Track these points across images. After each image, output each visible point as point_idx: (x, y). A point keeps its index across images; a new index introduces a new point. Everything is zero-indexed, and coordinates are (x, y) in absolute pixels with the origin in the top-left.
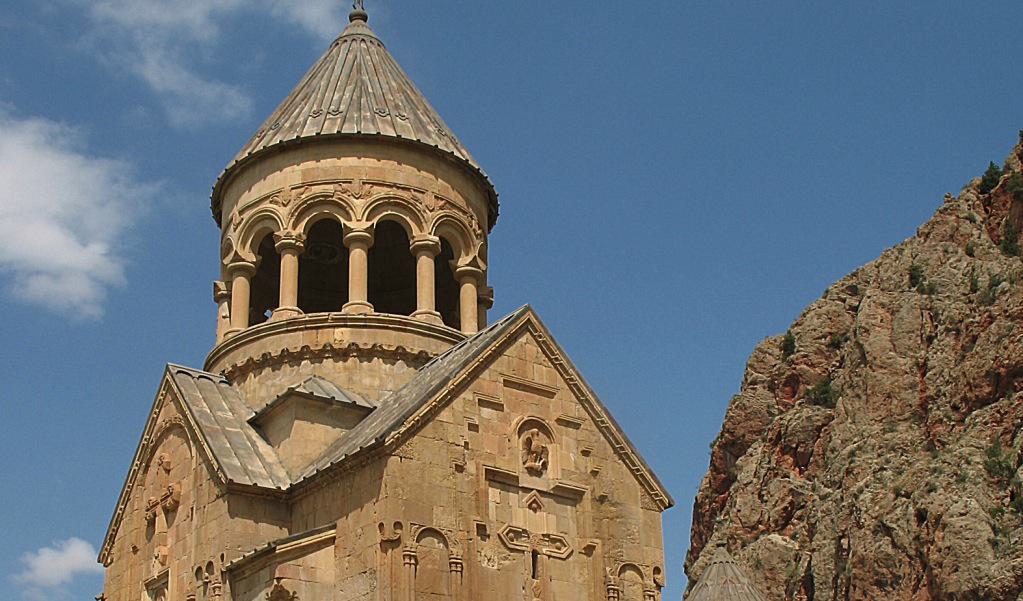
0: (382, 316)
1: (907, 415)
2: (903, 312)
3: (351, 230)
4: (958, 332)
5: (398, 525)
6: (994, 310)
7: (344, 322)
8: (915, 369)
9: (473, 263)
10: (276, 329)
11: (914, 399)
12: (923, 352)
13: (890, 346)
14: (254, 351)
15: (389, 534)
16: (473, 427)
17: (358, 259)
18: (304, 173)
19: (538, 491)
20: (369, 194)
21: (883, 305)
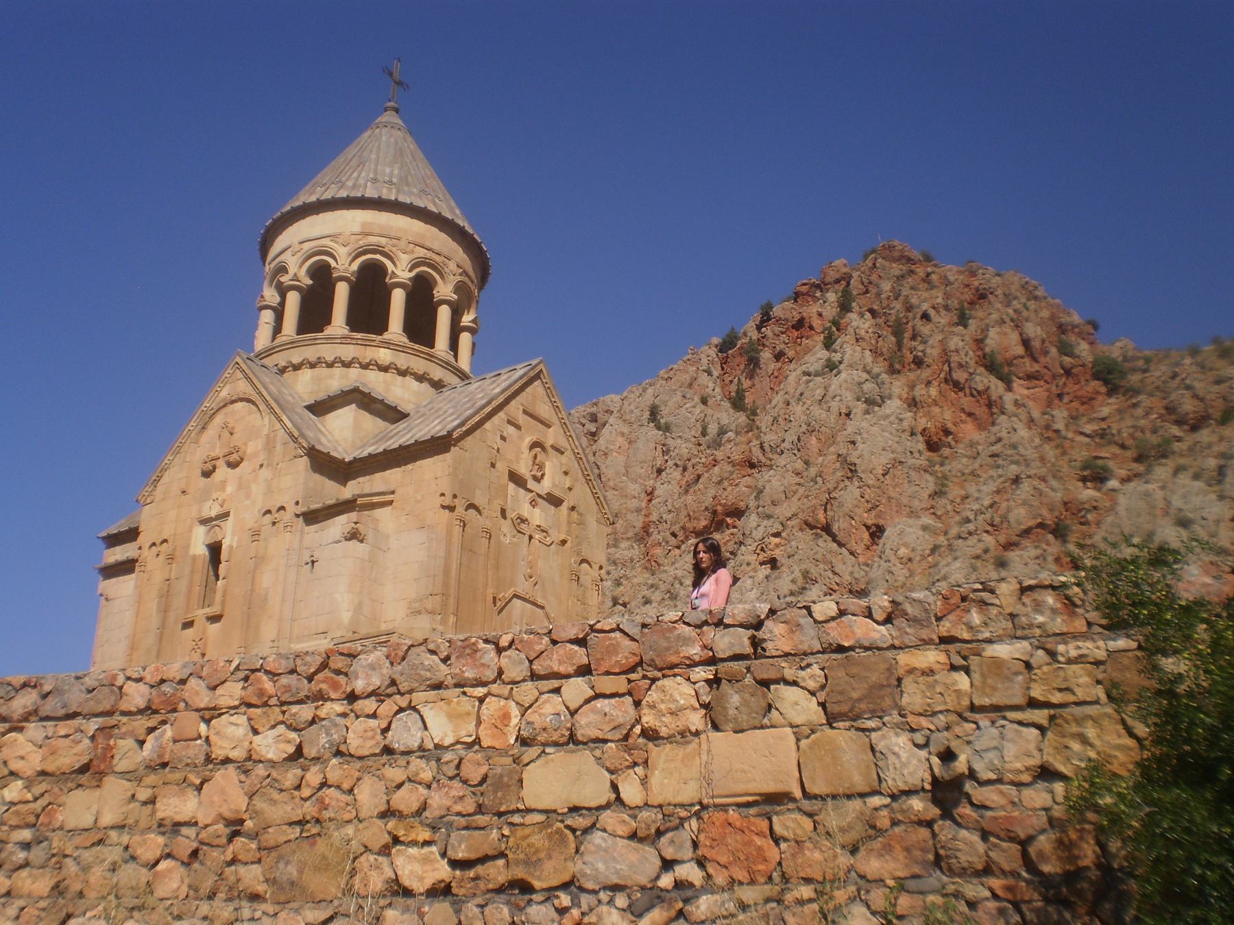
0: (417, 346)
1: (630, 534)
2: (640, 444)
3: (397, 276)
4: (685, 469)
5: (455, 496)
6: (719, 454)
7: (387, 345)
8: (643, 495)
9: (474, 321)
10: (331, 340)
11: (639, 524)
12: (652, 482)
13: (624, 471)
14: (310, 353)
15: (447, 501)
16: (503, 438)
17: (398, 299)
18: (364, 224)
19: (539, 496)
20: (412, 252)
21: (623, 434)
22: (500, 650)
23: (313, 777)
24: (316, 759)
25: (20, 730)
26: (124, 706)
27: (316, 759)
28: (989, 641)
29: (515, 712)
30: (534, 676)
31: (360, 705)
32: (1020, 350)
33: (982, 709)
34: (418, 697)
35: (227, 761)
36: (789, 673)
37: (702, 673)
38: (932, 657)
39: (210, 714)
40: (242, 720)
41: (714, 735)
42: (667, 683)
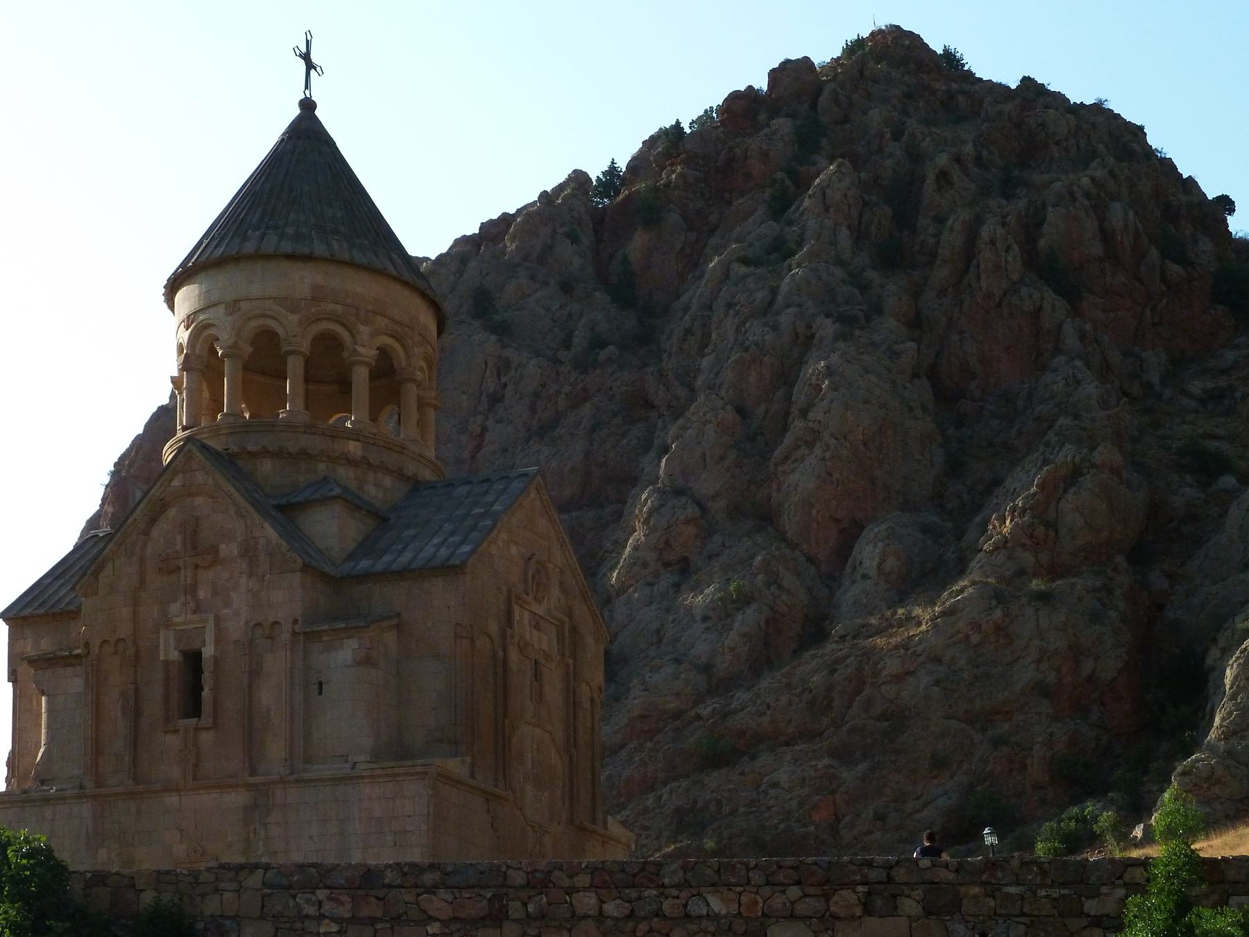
22: (748, 870)
23: (643, 927)
24: (645, 918)
25: (434, 894)
26: (509, 883)
27: (645, 918)
28: (1006, 885)
29: (760, 900)
30: (768, 883)
31: (667, 892)
32: (1097, 249)
33: (1000, 915)
34: (702, 889)
35: (586, 917)
36: (907, 892)
37: (860, 889)
38: (976, 890)
39: (570, 891)
40: (593, 895)
41: (868, 919)
42: (843, 892)
